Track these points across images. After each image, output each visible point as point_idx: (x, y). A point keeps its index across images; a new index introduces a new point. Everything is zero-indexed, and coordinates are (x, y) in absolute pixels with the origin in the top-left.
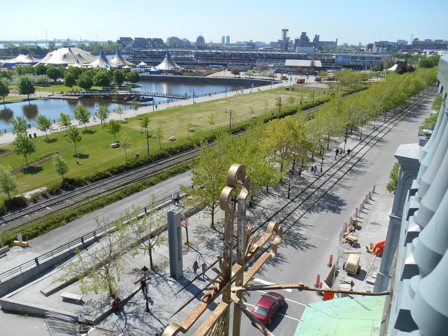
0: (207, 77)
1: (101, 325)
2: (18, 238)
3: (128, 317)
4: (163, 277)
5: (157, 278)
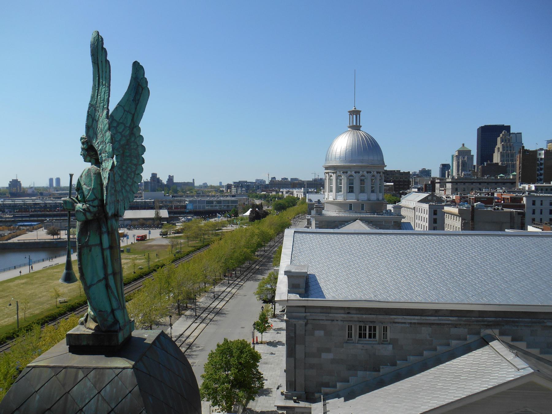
0: (9, 241)
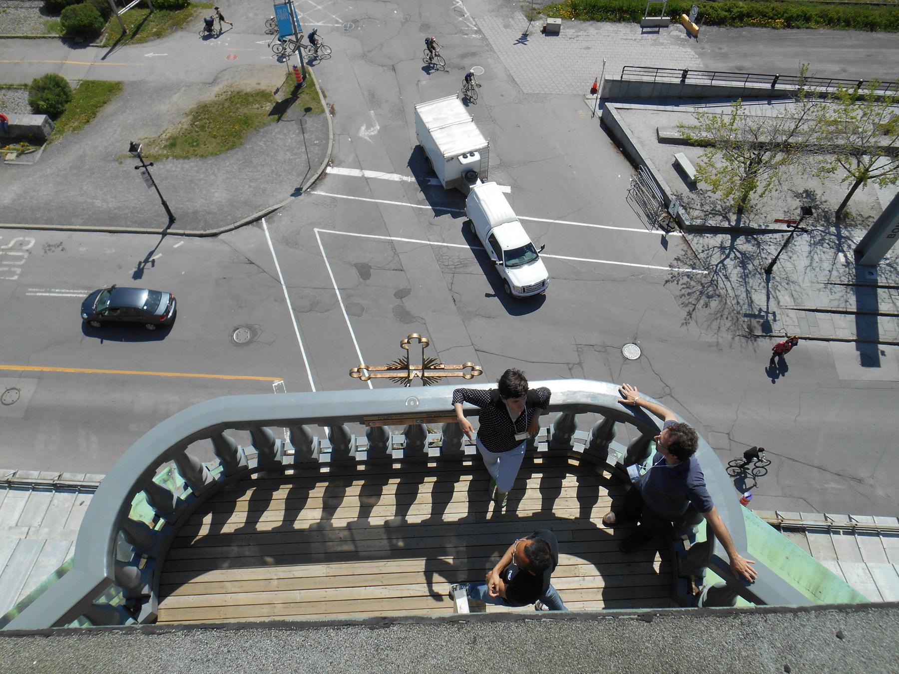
1: (689, 237)
2: (692, 12)
3: (732, 255)
4: (839, 240)
5: (829, 233)
